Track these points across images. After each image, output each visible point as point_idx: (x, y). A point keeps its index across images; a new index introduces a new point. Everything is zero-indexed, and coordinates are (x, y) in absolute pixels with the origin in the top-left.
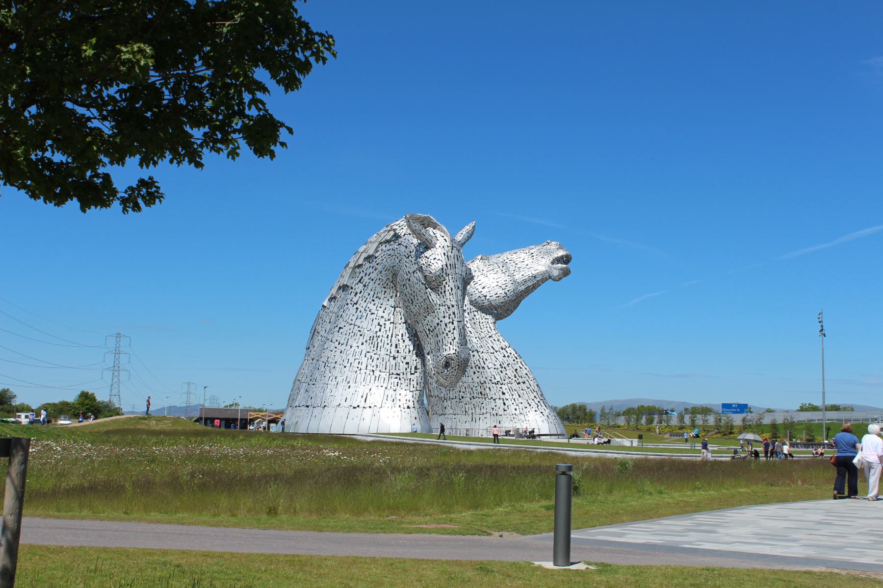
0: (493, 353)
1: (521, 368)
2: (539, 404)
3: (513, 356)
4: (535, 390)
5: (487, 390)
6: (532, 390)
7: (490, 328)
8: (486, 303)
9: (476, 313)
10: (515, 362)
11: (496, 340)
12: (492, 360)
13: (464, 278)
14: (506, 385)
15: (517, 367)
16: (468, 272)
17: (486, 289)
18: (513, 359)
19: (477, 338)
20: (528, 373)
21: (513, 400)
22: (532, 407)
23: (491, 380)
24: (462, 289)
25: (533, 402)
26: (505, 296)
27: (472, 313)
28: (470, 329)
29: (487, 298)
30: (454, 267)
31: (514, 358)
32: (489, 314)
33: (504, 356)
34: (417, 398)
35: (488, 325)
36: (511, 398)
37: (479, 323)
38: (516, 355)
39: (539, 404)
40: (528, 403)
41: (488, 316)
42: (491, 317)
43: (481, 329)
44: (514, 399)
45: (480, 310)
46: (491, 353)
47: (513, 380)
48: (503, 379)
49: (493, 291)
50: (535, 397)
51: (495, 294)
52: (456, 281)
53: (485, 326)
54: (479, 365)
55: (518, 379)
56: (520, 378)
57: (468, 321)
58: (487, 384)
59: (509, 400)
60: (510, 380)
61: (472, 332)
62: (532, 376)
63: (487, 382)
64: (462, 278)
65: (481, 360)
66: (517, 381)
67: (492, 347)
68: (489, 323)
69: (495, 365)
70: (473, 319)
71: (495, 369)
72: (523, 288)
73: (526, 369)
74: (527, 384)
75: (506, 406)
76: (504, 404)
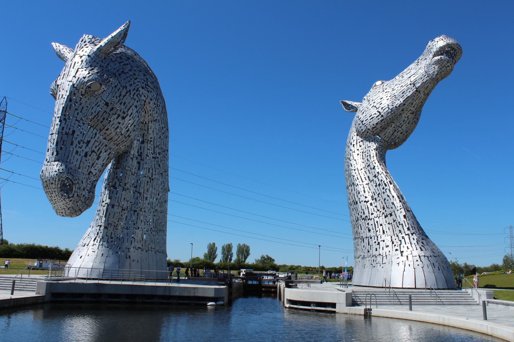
0: (369, 183)
1: (388, 196)
2: (403, 241)
3: (383, 184)
4: (402, 222)
5: (360, 227)
6: (398, 223)
7: (370, 156)
8: (364, 129)
9: (361, 143)
10: (384, 190)
11: (372, 168)
12: (365, 192)
13: (73, 85)
14: (373, 220)
15: (384, 196)
16: (81, 77)
17: (364, 114)
18: (382, 187)
19: (356, 170)
20: (395, 203)
21: (376, 237)
22: (395, 245)
23: (361, 216)
24: (66, 97)
25: (397, 238)
26: (378, 116)
27: (358, 144)
28: (351, 162)
29: (363, 123)
30: (67, 75)
31: (384, 185)
32: (372, 141)
33: (376, 186)
34: (96, 235)
35: (369, 154)
36: (375, 234)
37: (363, 153)
38: (385, 182)
39: (403, 241)
40: (392, 240)
41: (371, 143)
42: (373, 143)
43: (363, 159)
44: (377, 237)
45: (365, 140)
46: (366, 184)
47: (382, 213)
48: (370, 213)
49: (368, 114)
50: (400, 231)
51: (370, 117)
52: (63, 89)
53: (366, 156)
54: (354, 200)
55: (386, 211)
56: (387, 210)
57: (352, 154)
58: (359, 221)
59: (373, 238)
60: (378, 213)
61: (353, 165)
62: (399, 206)
63: (359, 219)
64: (71, 84)
65: (355, 194)
66: (385, 212)
67: (368, 177)
68: (371, 151)
69: (366, 197)
70: (358, 150)
71: (365, 202)
72: (402, 100)
73: (393, 197)
74: (393, 217)
75: (370, 246)
76: (369, 245)
